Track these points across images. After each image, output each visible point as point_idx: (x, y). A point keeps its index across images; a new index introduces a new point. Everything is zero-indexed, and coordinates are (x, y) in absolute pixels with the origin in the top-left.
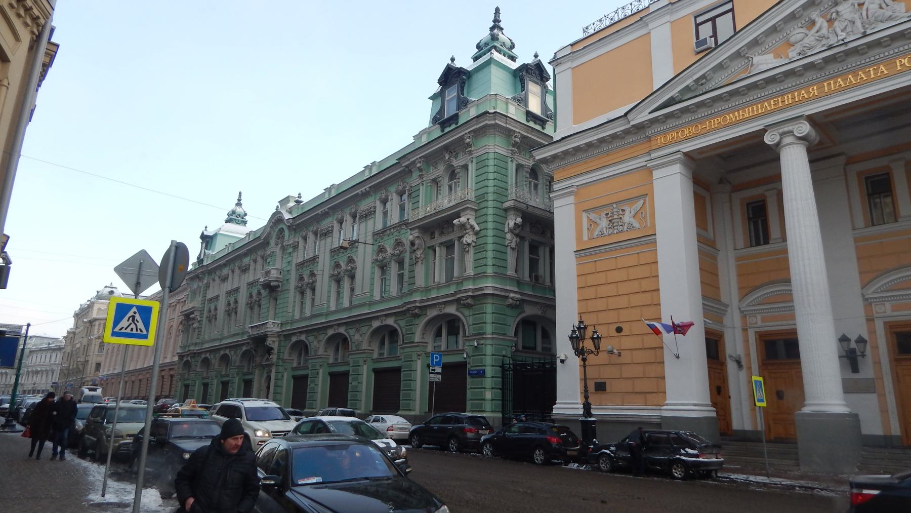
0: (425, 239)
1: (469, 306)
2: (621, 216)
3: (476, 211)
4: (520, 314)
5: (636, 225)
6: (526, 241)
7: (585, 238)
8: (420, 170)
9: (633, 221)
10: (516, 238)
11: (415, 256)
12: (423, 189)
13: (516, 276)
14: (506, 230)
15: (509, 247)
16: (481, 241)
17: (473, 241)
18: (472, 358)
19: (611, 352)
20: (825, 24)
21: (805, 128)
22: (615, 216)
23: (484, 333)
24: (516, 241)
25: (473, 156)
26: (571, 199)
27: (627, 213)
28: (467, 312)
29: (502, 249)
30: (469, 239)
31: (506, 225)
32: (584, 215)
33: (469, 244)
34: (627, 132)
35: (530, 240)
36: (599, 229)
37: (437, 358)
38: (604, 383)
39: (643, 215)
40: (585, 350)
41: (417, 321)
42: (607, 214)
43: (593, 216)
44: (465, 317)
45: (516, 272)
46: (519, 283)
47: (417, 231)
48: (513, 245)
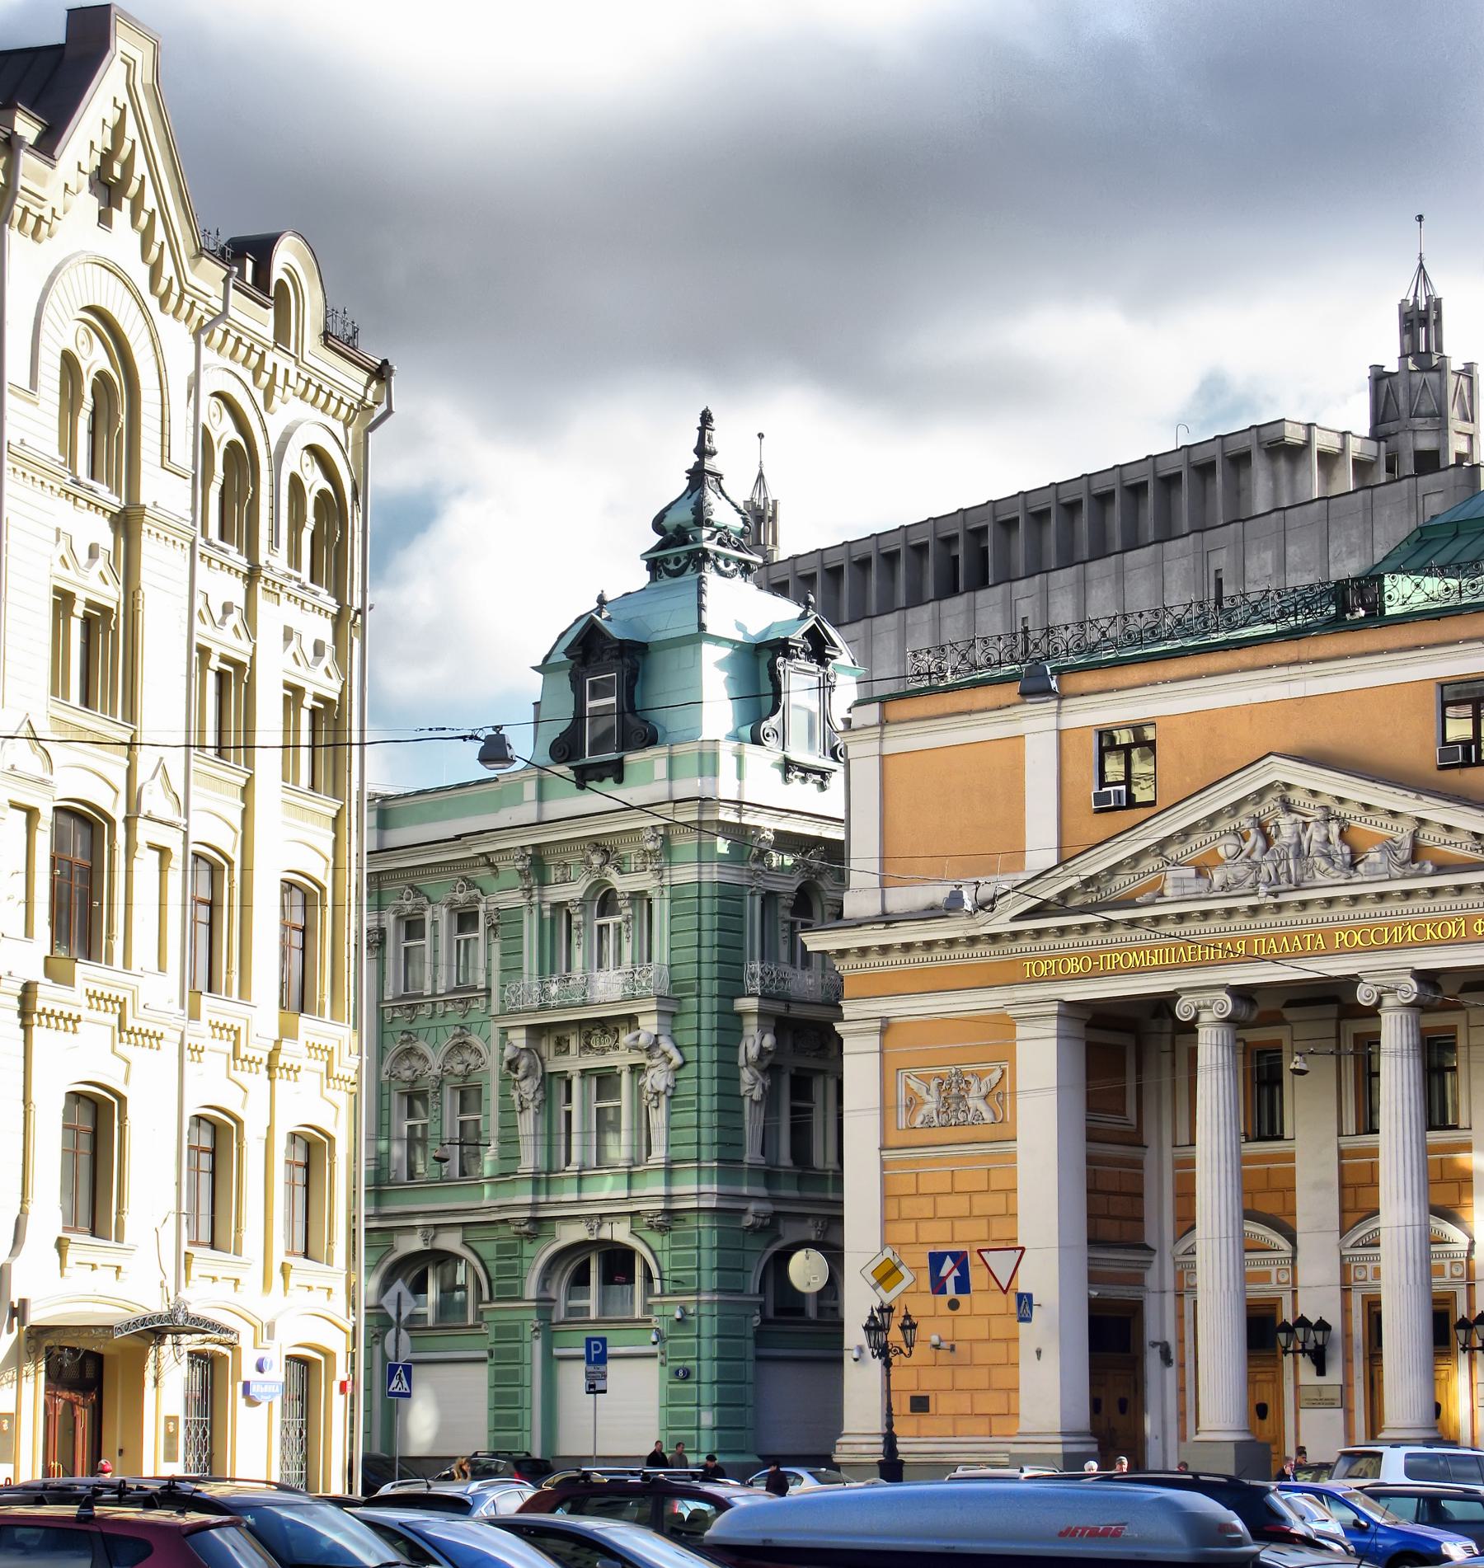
1: (663, 1229)
3: (674, 1015)
5: (988, 1116)
6: (784, 1073)
9: (982, 1106)
10: (763, 1076)
11: (520, 1096)
13: (763, 1162)
14: (742, 1061)
17: (668, 1086)
18: (669, 1341)
20: (1260, 843)
21: (1227, 1003)
22: (954, 1091)
24: (763, 1085)
27: (974, 1087)
30: (658, 1078)
35: (793, 1071)
38: (927, 1398)
39: (1001, 1098)
40: (890, 1347)
41: (528, 1249)
45: (763, 1153)
46: (769, 1176)
48: (757, 1094)
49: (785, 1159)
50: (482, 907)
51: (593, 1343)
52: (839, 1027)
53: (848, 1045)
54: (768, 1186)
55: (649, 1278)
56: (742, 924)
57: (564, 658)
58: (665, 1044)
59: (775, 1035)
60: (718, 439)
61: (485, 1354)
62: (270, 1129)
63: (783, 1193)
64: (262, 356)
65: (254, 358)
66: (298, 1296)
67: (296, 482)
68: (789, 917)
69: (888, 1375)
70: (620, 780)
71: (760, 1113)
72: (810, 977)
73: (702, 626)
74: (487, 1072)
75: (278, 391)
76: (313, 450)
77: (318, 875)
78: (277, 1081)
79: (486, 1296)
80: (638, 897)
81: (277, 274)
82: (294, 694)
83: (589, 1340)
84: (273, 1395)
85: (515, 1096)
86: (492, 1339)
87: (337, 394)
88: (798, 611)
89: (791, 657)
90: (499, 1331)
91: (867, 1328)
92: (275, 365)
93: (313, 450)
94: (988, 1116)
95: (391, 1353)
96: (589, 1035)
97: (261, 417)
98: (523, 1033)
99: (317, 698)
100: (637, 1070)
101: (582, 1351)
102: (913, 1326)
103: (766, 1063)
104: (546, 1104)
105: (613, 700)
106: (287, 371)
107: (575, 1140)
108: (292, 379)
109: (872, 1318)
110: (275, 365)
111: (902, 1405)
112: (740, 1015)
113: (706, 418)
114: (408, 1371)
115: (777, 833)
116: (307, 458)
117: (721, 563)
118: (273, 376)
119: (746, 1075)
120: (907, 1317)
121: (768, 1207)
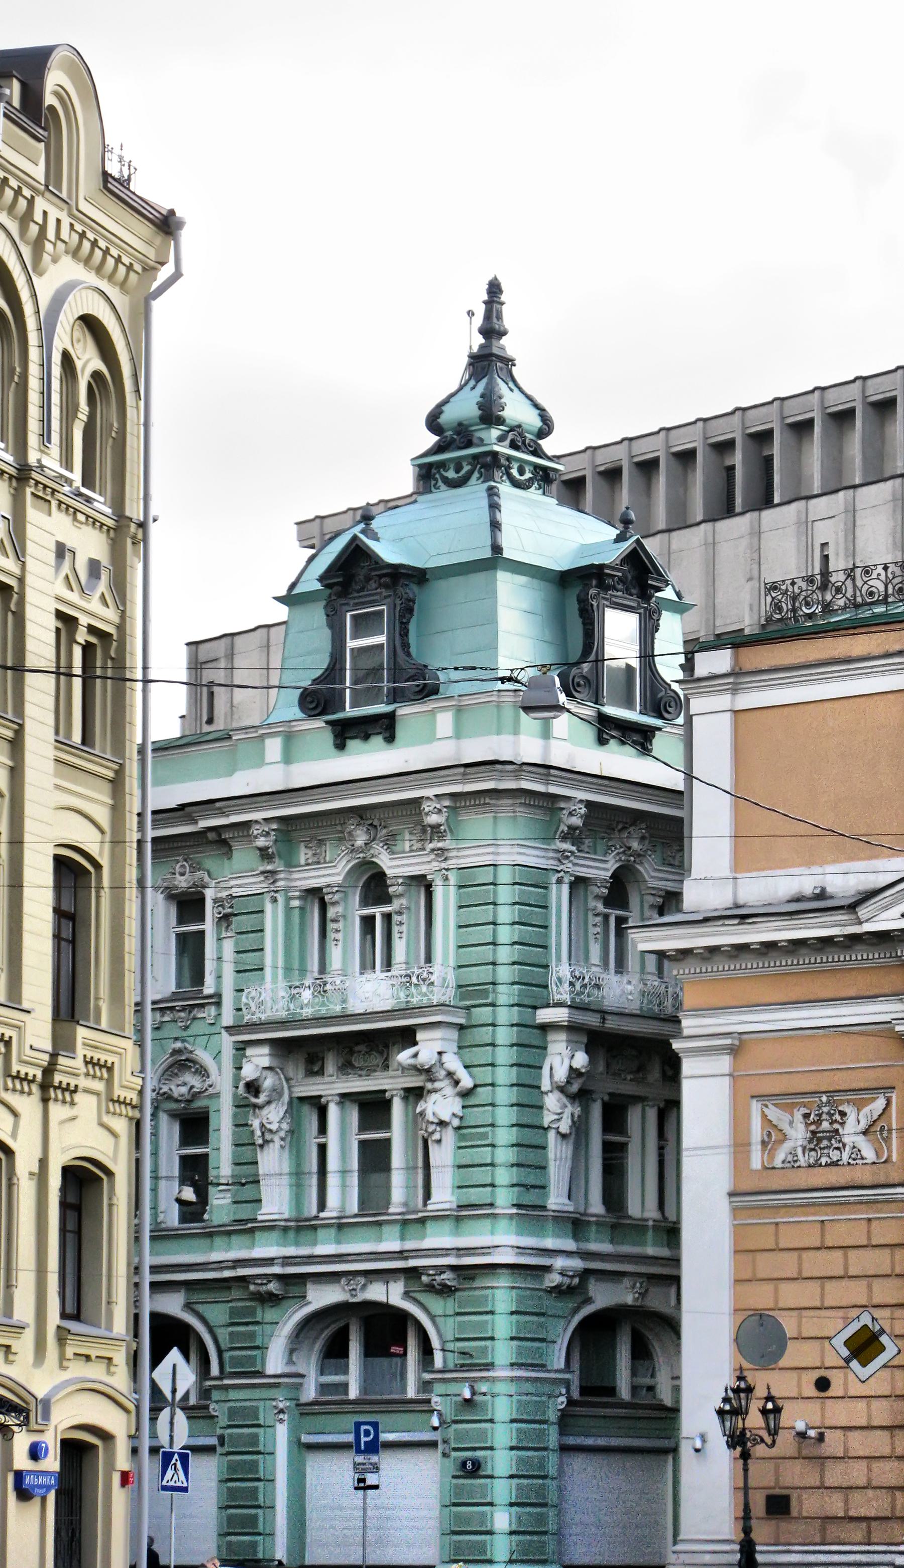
0: (291, 1074)
1: (445, 1291)
2: (836, 1126)
3: (461, 1027)
4: (575, 1311)
5: (869, 1154)
6: (594, 1101)
7: (756, 1162)
8: (264, 854)
9: (861, 1142)
10: (572, 1104)
11: (262, 1125)
12: (275, 912)
13: (571, 1209)
14: (546, 1085)
15: (552, 1135)
16: (477, 1116)
17: (454, 1115)
18: (455, 1426)
19: (802, 1435)
22: (825, 1125)
23: (489, 1366)
24: (572, 1115)
25: (452, 863)
26: (724, 1063)
27: (851, 1119)
28: (437, 1305)
29: (531, 1136)
31: (546, 1071)
32: (755, 1107)
33: (442, 1124)
34: (855, 939)
35: (606, 1098)
36: (787, 1146)
37: (367, 1433)
39: (885, 1134)
41: (270, 1314)
42: (806, 1116)
43: (773, 1113)
44: (432, 1318)
45: (569, 1198)
47: (266, 1050)
48: (565, 1127)
49: (597, 1207)
50: (209, 894)
51: (363, 1428)
52: (676, 1045)
53: (688, 1067)
54: (576, 1237)
55: (426, 1350)
56: (547, 917)
57: (318, 586)
58: (453, 1063)
59: (587, 1052)
60: (510, 317)
61: (213, 1441)
62: (43, 1163)
63: (593, 1247)
64: (31, 202)
65: (22, 204)
66: (78, 1370)
67: (67, 358)
68: (600, 907)
69: (746, 1470)
70: (390, 739)
71: (567, 1150)
72: (629, 983)
73: (497, 549)
74: (217, 1095)
75: (49, 247)
76: (89, 322)
77: (93, 849)
78: (52, 1105)
79: (215, 1370)
80: (422, 883)
81: (49, 100)
82: (67, 621)
83: (358, 1425)
84: (48, 1488)
85: (256, 1124)
86: (223, 1421)
87: (114, 252)
88: (613, 533)
89: (607, 588)
90: (232, 1413)
91: (721, 1413)
92: (45, 213)
93: (89, 322)
94: (869, 1154)
95: (164, 1439)
96: (351, 1052)
97: (30, 280)
98: (266, 1050)
99: (92, 629)
100: (415, 1094)
101: (350, 1438)
102: (777, 1410)
103: (575, 1088)
104: (294, 1134)
105: (381, 639)
106: (58, 221)
107: (333, 1181)
108: (65, 235)
109: (726, 1400)
110: (45, 213)
111: (758, 1506)
112: (545, 1028)
113: (494, 289)
114: (184, 1459)
115: (589, 804)
116: (80, 332)
117: (514, 472)
118: (43, 228)
119: (553, 1102)
120: (769, 1398)
121: (577, 1264)
